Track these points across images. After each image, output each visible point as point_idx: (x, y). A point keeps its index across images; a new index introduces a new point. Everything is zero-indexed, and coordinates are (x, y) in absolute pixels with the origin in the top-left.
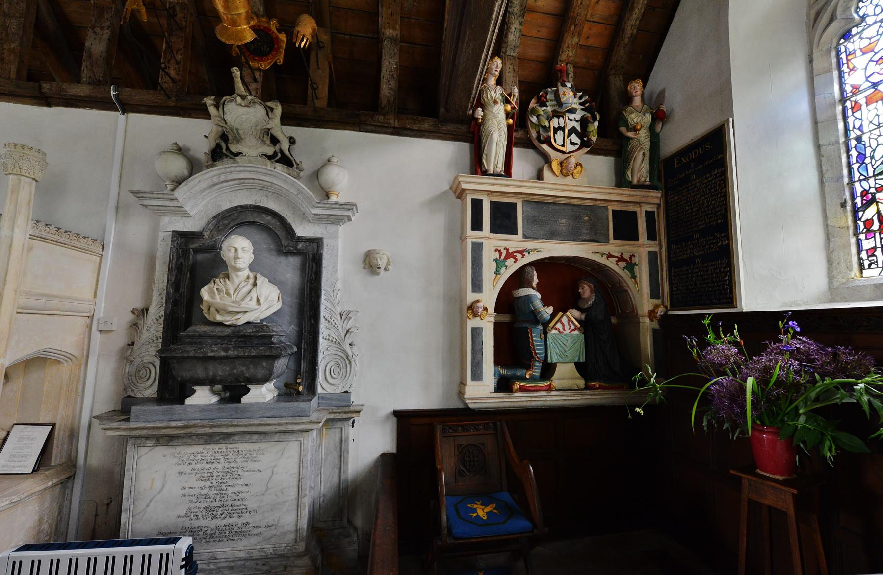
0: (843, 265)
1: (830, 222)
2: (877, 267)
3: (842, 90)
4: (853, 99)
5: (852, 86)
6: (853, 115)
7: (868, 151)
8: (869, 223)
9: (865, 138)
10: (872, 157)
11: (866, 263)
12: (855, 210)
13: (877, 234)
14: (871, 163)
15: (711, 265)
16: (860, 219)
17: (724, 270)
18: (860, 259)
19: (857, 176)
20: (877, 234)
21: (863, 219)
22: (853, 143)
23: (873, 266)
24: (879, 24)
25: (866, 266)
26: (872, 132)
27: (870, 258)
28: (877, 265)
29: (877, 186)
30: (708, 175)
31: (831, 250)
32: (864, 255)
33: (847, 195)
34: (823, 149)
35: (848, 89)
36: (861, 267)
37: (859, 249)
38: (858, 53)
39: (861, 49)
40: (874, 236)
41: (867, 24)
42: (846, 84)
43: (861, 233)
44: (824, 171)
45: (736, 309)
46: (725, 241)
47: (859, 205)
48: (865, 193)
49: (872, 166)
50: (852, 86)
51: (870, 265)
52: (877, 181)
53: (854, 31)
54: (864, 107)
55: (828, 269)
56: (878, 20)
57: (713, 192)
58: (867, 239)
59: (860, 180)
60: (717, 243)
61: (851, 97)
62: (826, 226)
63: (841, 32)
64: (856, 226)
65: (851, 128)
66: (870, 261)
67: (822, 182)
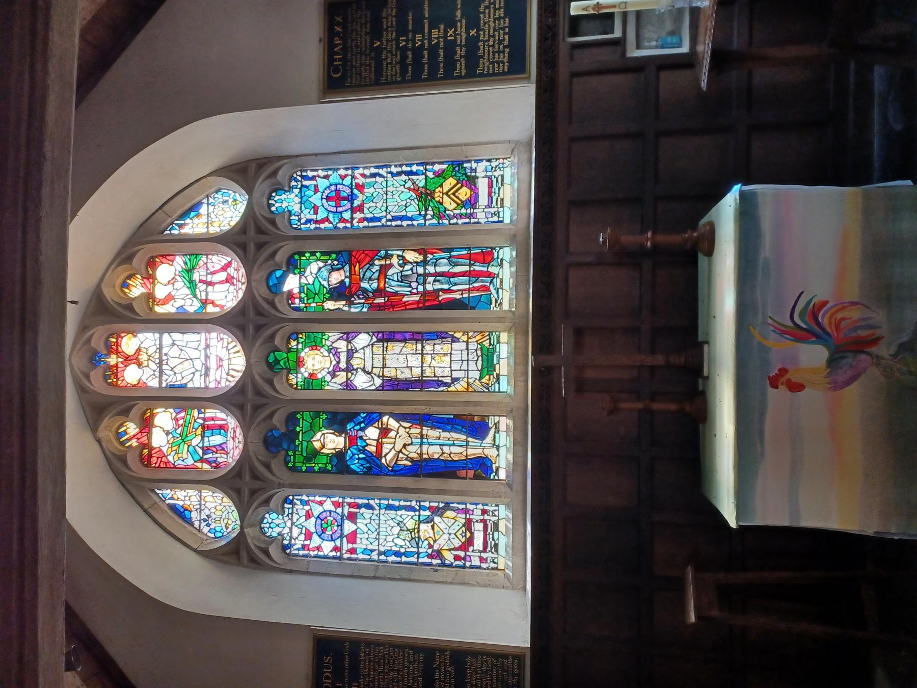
0: (490, 578)
1: (449, 580)
2: (498, 558)
3: (334, 558)
4: (344, 552)
5: (331, 551)
6: (357, 554)
7: (395, 548)
8: (457, 558)
9: (382, 549)
10: (402, 547)
11: (492, 565)
12: (443, 565)
13: (468, 553)
14: (405, 548)
15: (471, 679)
16: (452, 563)
17: (480, 662)
18: (488, 568)
19: (413, 559)
20: (468, 553)
21: (453, 561)
22: (383, 557)
23: (496, 561)
24: (294, 526)
25: (496, 565)
26: (380, 544)
27: (489, 561)
28: (495, 558)
29: (427, 547)
30: (362, 665)
31: (476, 584)
32: (484, 565)
33: (429, 568)
34: (378, 575)
35: (334, 553)
36: (497, 569)
37: (479, 567)
38: (307, 542)
39: (306, 539)
40: (470, 556)
41: (288, 533)
42: (327, 555)
43: (465, 564)
44: (400, 577)
45: (526, 654)
46: (446, 656)
47: (439, 562)
48: (430, 556)
49: (408, 548)
50: (331, 551)
51: (494, 563)
52: (423, 547)
53: (286, 542)
54: (355, 546)
55: (493, 587)
56: (290, 526)
57: (384, 661)
58: (471, 561)
59: (418, 558)
60: (445, 666)
61: (342, 554)
62: (451, 583)
63: (280, 550)
64: (457, 566)
65: (369, 557)
66: (491, 562)
67: (409, 580)
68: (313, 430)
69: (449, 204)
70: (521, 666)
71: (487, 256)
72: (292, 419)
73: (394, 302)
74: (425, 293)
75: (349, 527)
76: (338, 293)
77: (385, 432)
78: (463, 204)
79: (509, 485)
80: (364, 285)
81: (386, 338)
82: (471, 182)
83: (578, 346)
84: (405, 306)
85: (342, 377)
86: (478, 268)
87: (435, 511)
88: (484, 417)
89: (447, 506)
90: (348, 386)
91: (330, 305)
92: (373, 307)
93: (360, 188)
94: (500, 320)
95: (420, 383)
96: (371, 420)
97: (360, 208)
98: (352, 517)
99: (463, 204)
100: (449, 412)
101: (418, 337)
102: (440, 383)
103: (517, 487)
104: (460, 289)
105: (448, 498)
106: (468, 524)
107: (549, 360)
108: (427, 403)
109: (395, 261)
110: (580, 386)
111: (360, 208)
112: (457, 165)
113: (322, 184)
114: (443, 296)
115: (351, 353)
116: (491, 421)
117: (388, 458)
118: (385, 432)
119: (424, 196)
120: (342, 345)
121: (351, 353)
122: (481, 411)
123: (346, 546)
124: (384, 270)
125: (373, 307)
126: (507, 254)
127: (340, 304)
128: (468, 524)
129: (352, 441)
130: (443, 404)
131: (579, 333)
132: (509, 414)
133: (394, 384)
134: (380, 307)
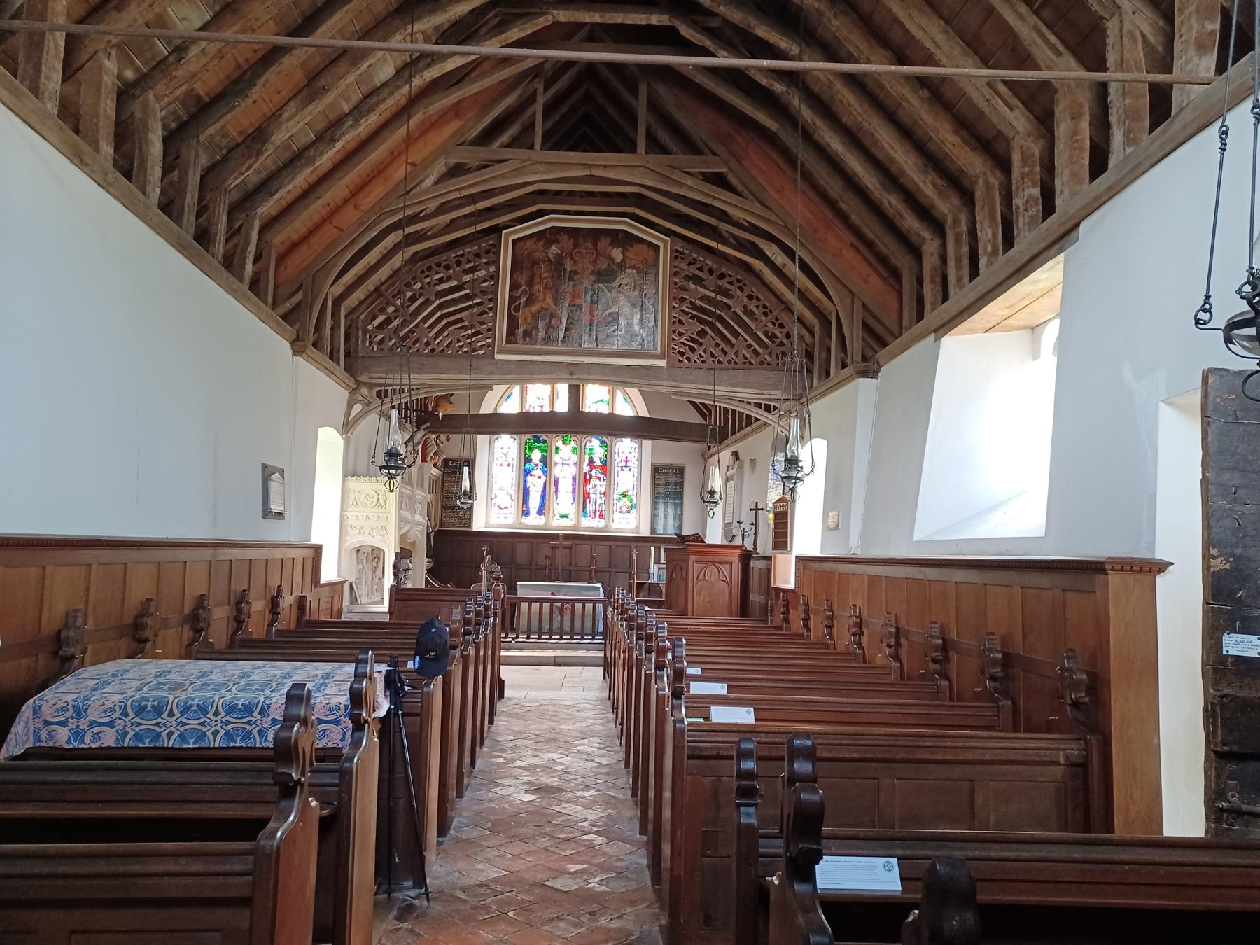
68: (539, 448)
69: (620, 504)
70: (467, 527)
71: (602, 516)
72: (545, 442)
73: (587, 482)
74: (589, 494)
75: (505, 464)
76: (591, 461)
77: (539, 477)
78: (621, 508)
79: (520, 523)
80: (594, 470)
81: (574, 479)
82: (628, 512)
83: (565, 548)
84: (585, 486)
85: (560, 461)
86: (598, 514)
87: (511, 496)
88: (544, 514)
89: (513, 500)
90: (556, 464)
91: (587, 457)
92: (586, 474)
93: (630, 470)
94: (578, 521)
95: (556, 491)
96: (544, 472)
97: (622, 470)
98: (509, 465)
99: (621, 508)
100: (546, 502)
101: (574, 491)
102: (557, 498)
103: (520, 526)
104: (590, 507)
105: (516, 500)
106: (506, 508)
107: (561, 539)
108: (550, 495)
109: (602, 483)
110: (554, 548)
111: (622, 470)
112: (633, 507)
113: (633, 454)
114: (588, 500)
115: (568, 465)
116: (543, 517)
117: (529, 478)
118: (539, 477)
119: (624, 495)
120: (571, 462)
121: (568, 465)
122: (547, 514)
123: (499, 463)
124: (599, 478)
125: (586, 474)
126: (601, 523)
127: (587, 462)
128: (506, 508)
129: (537, 465)
130: (549, 500)
131: (570, 548)
132: (546, 524)
133: (556, 482)
134: (585, 477)
